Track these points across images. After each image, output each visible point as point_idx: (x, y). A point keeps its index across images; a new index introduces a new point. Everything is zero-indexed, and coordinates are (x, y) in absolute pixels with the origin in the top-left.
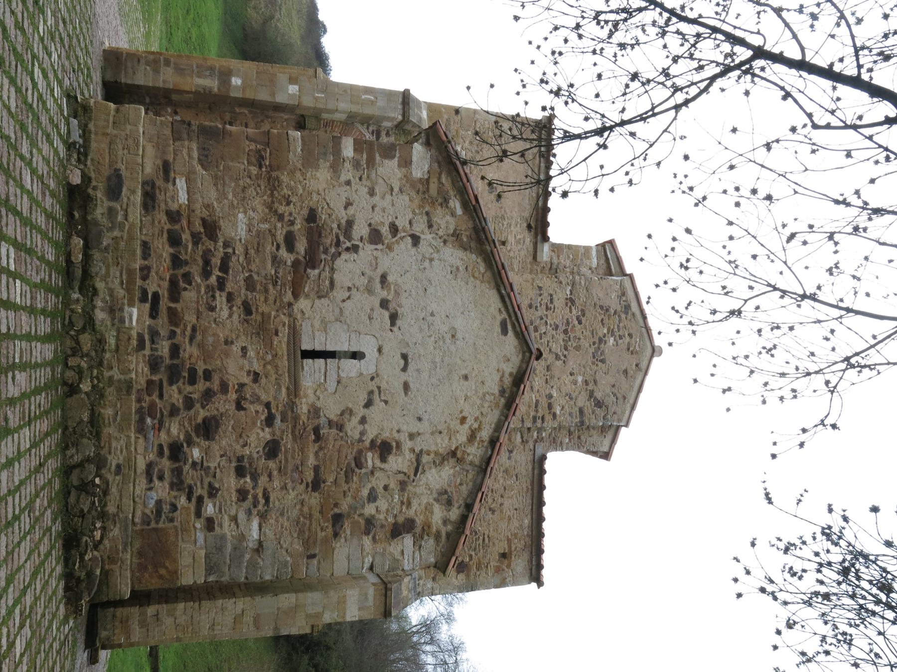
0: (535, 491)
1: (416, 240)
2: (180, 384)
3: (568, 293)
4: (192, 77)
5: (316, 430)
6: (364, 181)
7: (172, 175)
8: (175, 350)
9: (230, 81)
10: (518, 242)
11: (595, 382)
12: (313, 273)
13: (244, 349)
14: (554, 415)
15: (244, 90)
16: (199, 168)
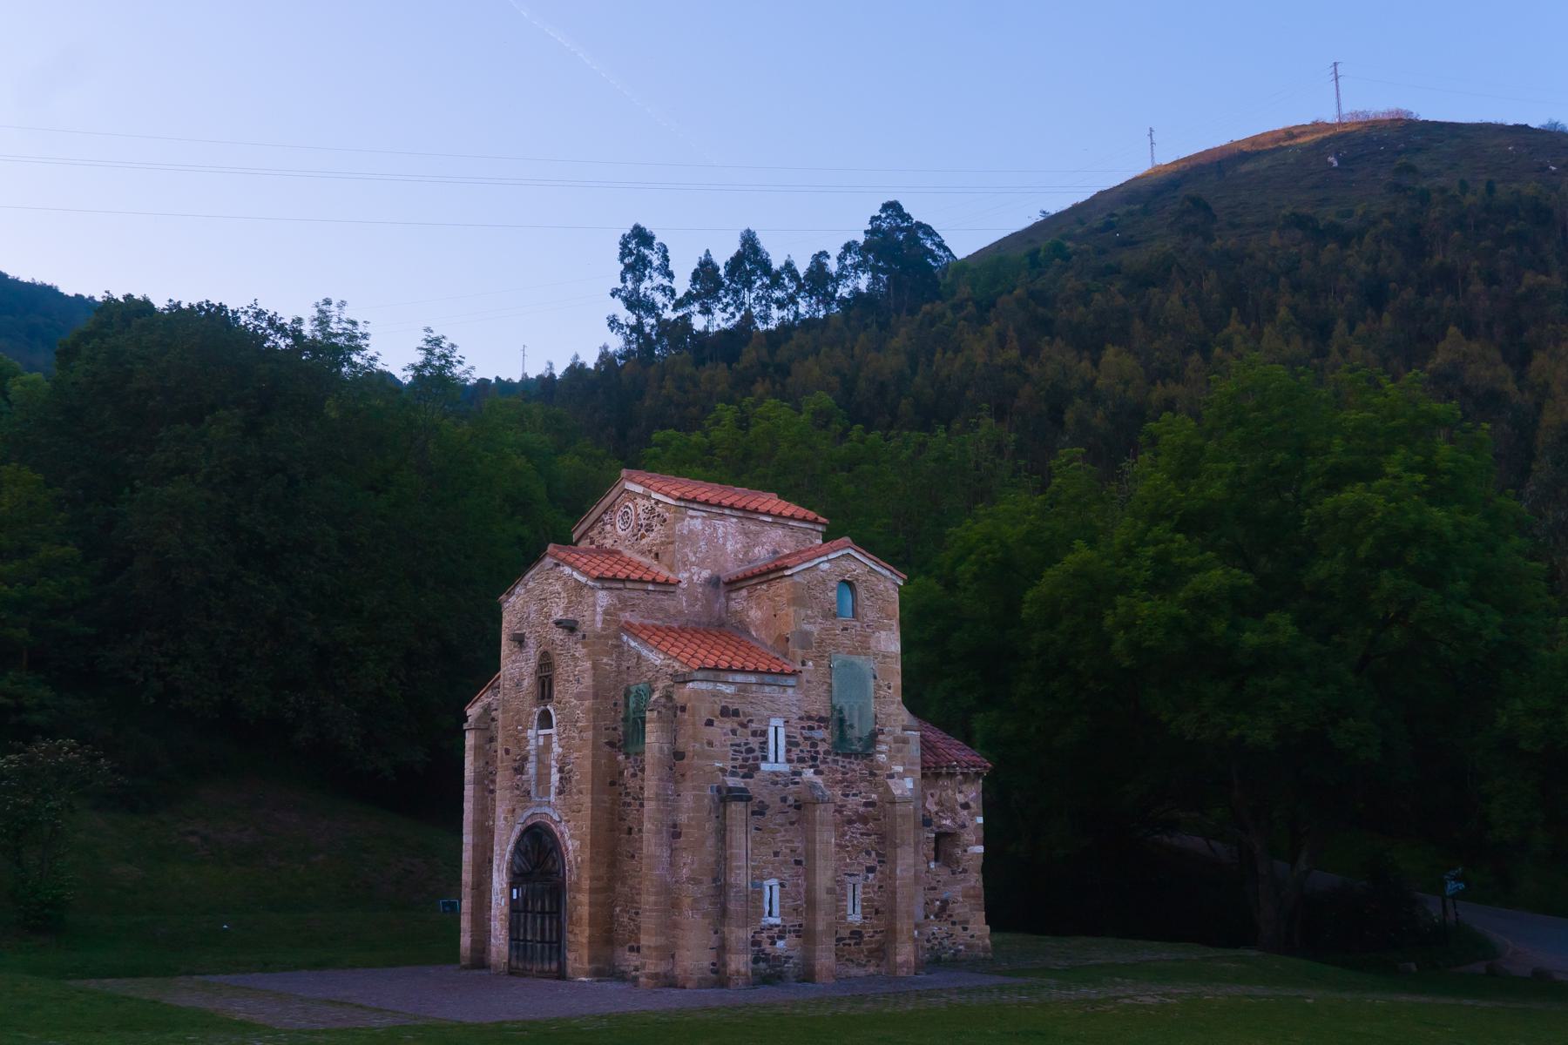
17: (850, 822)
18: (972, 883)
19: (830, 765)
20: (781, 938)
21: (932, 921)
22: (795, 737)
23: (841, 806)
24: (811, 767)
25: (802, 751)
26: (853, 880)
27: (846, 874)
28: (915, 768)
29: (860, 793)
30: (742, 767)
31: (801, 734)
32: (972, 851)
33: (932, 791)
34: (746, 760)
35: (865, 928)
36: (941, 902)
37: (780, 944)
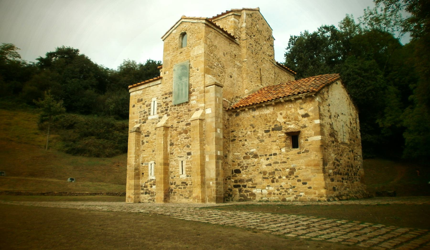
0: (282, 68)
1: (329, 105)
5: (351, 140)
6: (324, 118)
8: (346, 174)
9: (219, 156)
12: (336, 137)
17: (180, 133)
18: (312, 158)
19: (173, 111)
20: (154, 185)
21: (284, 180)
22: (160, 103)
23: (176, 128)
24: (166, 113)
25: (162, 108)
26: (181, 159)
27: (178, 157)
28: (211, 103)
29: (184, 120)
30: (143, 119)
31: (163, 101)
32: (311, 140)
33: (281, 112)
34: (144, 116)
35: (187, 180)
36: (290, 169)
37: (154, 187)
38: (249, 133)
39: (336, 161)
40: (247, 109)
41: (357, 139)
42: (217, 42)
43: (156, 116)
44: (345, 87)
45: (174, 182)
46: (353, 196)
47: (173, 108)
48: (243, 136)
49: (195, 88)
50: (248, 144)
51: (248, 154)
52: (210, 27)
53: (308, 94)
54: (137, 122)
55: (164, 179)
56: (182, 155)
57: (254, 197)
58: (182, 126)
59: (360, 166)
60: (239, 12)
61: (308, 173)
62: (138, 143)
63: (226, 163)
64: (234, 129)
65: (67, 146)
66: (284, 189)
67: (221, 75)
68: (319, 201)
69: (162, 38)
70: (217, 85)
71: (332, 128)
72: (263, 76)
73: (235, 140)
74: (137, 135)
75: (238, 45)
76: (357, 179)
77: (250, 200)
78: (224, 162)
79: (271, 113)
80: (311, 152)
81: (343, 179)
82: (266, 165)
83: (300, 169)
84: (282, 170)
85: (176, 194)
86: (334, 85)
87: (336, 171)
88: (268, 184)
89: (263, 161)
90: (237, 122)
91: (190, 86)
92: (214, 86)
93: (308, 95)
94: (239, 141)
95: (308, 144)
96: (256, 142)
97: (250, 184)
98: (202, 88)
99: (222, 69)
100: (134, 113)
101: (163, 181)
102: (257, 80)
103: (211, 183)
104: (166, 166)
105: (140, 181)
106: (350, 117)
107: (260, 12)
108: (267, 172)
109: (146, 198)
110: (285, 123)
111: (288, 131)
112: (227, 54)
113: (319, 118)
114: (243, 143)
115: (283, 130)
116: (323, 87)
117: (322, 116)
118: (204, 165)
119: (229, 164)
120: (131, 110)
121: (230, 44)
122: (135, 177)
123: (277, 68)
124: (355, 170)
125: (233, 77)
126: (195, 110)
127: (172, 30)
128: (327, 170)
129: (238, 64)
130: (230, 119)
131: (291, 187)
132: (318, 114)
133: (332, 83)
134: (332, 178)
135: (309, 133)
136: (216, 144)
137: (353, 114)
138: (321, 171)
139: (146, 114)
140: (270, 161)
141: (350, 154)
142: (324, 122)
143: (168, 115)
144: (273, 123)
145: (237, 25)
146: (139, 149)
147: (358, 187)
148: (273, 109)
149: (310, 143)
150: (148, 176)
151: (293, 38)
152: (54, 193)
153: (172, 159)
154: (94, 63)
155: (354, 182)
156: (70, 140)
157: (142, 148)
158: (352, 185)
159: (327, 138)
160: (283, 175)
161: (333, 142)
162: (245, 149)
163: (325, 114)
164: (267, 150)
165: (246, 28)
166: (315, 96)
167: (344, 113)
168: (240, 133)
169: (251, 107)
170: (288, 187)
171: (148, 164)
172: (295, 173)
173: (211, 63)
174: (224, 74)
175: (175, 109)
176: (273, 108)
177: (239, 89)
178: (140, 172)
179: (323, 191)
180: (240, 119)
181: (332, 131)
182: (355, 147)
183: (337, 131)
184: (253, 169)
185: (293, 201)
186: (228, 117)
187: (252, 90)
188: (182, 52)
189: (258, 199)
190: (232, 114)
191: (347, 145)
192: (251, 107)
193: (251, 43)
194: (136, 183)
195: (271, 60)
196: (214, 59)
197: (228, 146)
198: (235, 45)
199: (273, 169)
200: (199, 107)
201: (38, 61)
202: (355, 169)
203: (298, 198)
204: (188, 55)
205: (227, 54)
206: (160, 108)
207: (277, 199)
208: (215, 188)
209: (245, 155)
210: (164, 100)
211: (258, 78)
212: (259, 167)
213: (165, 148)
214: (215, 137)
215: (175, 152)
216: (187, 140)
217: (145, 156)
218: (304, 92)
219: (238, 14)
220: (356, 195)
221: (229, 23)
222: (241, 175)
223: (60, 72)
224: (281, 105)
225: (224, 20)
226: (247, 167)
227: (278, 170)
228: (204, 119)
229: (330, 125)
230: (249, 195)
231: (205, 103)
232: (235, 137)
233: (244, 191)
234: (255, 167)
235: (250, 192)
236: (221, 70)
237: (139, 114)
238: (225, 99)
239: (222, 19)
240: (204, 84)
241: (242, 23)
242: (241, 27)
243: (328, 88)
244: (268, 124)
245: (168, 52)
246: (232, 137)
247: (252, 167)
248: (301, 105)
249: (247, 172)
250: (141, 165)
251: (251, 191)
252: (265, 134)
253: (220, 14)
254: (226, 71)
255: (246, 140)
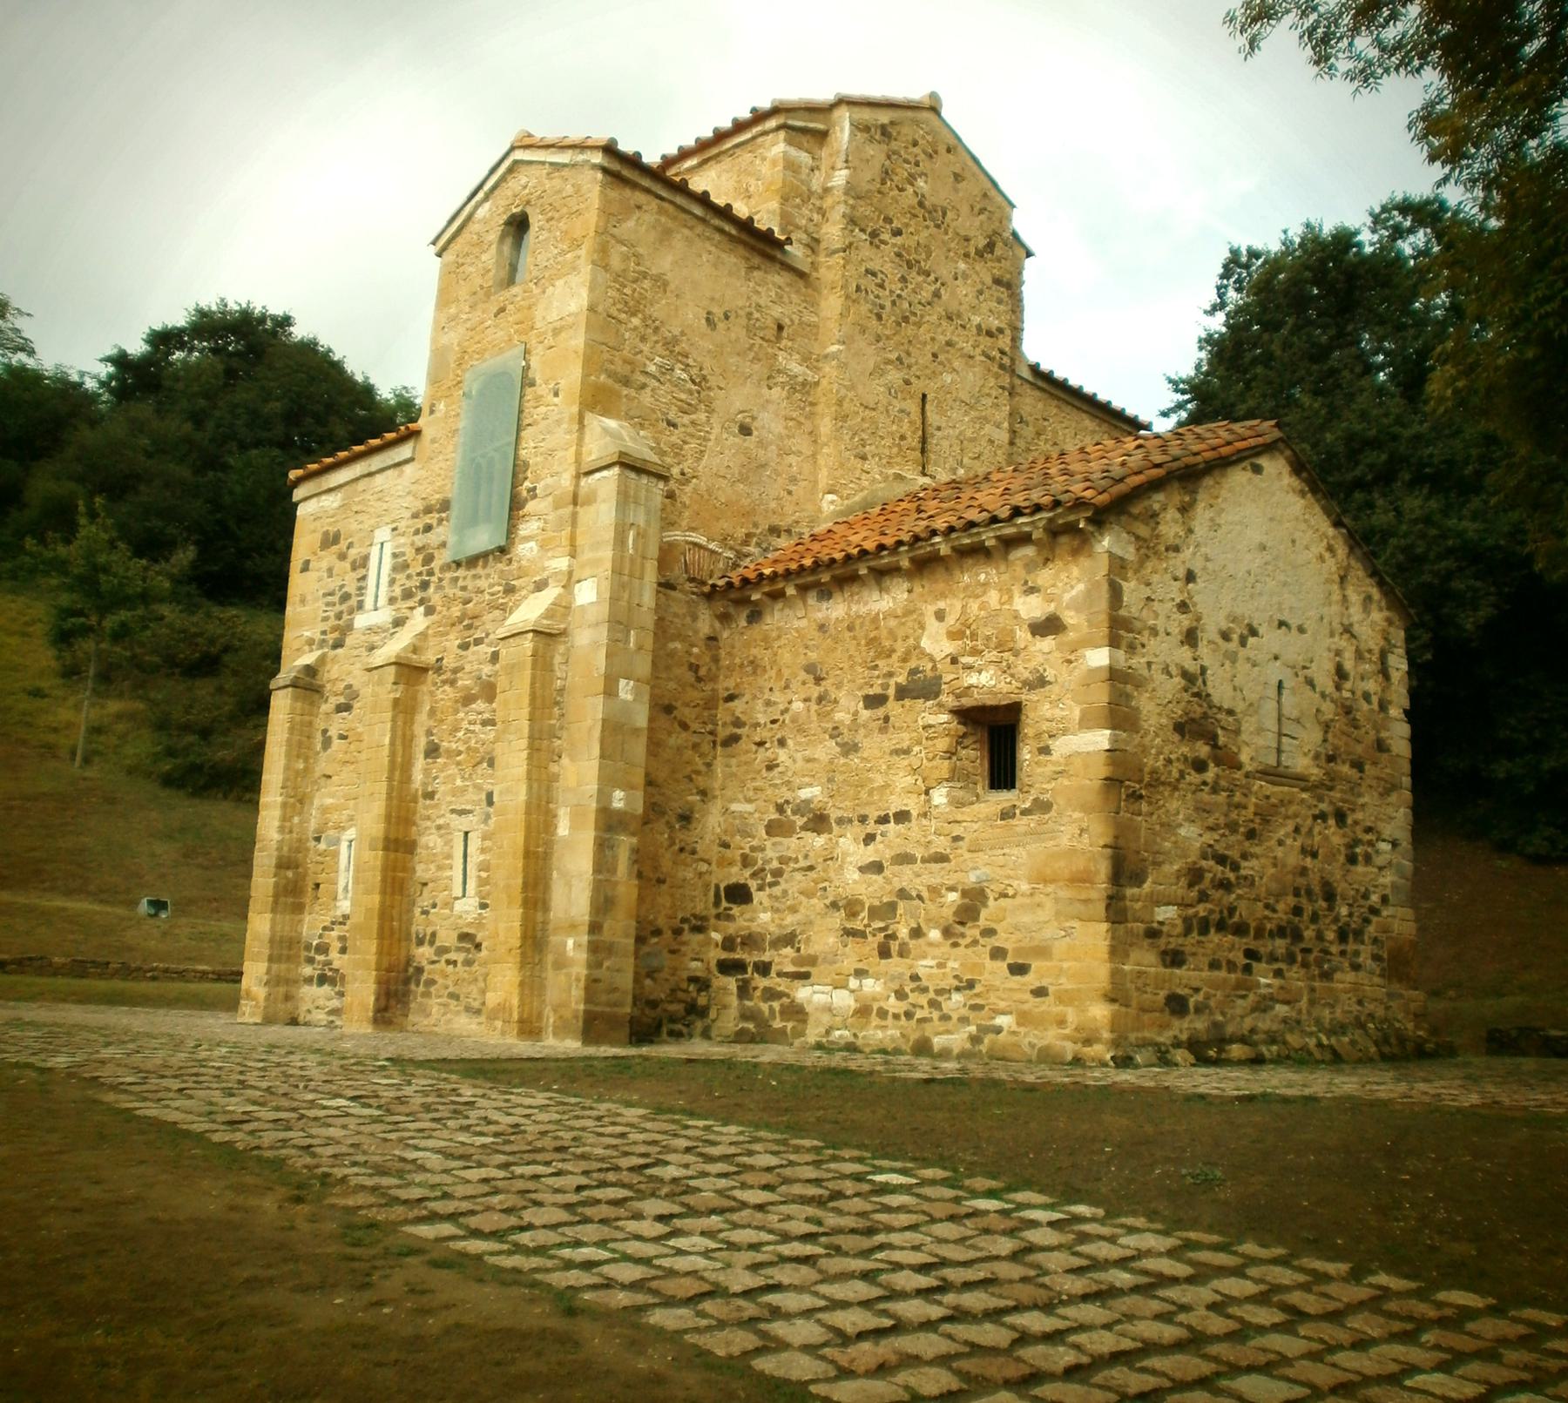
0: (1062, 395)
1: (1190, 577)
2: (1302, 926)
3: (864, 237)
4: (616, 883)
5: (1331, 759)
6: (1144, 640)
7: (1155, 925)
8: (1281, 932)
9: (618, 812)
10: (778, 300)
11: (967, 240)
12: (1222, 740)
13: (1280, 843)
14: (1000, 331)
15: (632, 788)
16: (1147, 886)
17: (468, 700)
18: (1065, 841)
21: (931, 944)
22: (403, 554)
23: (455, 671)
24: (422, 602)
27: (453, 811)
28: (600, 554)
29: (488, 635)
30: (334, 629)
32: (1066, 751)
33: (941, 604)
34: (339, 616)
36: (965, 894)
38: (798, 706)
39: (1212, 863)
40: (791, 591)
41: (1385, 756)
42: (670, 258)
43: (384, 616)
44: (1314, 490)
45: (429, 931)
46: (1312, 1042)
47: (448, 575)
48: (774, 722)
49: (538, 479)
50: (789, 763)
51: (789, 812)
52: (634, 186)
53: (1059, 516)
54: (310, 642)
55: (385, 915)
56: (468, 802)
57: (800, 1027)
58: (476, 662)
59: (1388, 891)
60: (821, 116)
61: (1043, 915)
62: (301, 746)
63: (682, 850)
64: (737, 685)
65: (170, 753)
66: (925, 990)
67: (686, 419)
68: (1077, 1061)
69: (434, 243)
70: (628, 464)
71: (1197, 695)
72: (939, 429)
73: (735, 739)
74: (299, 704)
75: (802, 275)
76: (1365, 958)
77: (780, 1037)
78: (672, 843)
79: (899, 612)
80: (1060, 814)
81: (1251, 954)
82: (862, 869)
83: (1006, 896)
84: (925, 894)
85: (432, 989)
86: (1239, 477)
87: (1202, 914)
88: (860, 966)
89: (849, 845)
90: (754, 651)
91: (518, 470)
92: (616, 470)
93: (1061, 521)
94: (754, 748)
95: (1051, 768)
96: (826, 750)
97: (784, 959)
98: (566, 481)
99: (690, 392)
100: (303, 601)
101: (376, 921)
102: (895, 450)
103: (570, 943)
104: (399, 855)
105: (300, 921)
106: (1342, 642)
107: (944, 114)
108: (862, 903)
109: (321, 1002)
110: (954, 661)
111: (967, 702)
112: (727, 317)
113: (1106, 641)
114: (769, 754)
115: (943, 698)
116: (1155, 485)
117: (1130, 631)
118: (547, 856)
119: (701, 854)
120: (298, 584)
121: (752, 268)
122: (276, 902)
123: (1037, 393)
124: (1350, 915)
125: (755, 433)
126: (532, 587)
127: (473, 202)
128: (1138, 905)
129: (796, 368)
130: (725, 634)
131: (956, 983)
132: (1103, 618)
133: (1222, 464)
134: (1171, 946)
135: (1058, 713)
136: (602, 756)
137: (1363, 631)
138: (1100, 909)
139: (349, 601)
140: (877, 851)
141: (1316, 830)
142: (1138, 662)
143: (430, 611)
144: (904, 660)
145: (803, 177)
146: (306, 770)
147: (1360, 1002)
148: (910, 591)
149: (1057, 763)
150: (335, 899)
151: (1244, 259)
152: (50, 964)
153: (429, 823)
154: (359, 378)
155: (1338, 976)
156: (186, 728)
157: (322, 765)
158: (1313, 990)
159: (1158, 741)
160: (929, 920)
161: (1200, 766)
162: (775, 786)
163: (1151, 622)
164: (871, 793)
165: (846, 193)
166: (1090, 528)
167: (1294, 622)
168: (759, 705)
169: (810, 579)
170: (944, 985)
171: (337, 842)
172: (984, 914)
173: (625, 361)
174: (702, 416)
175: (456, 579)
176: (906, 585)
177: (790, 493)
178: (305, 875)
179: (1100, 1012)
180: (766, 639)
181: (1197, 711)
182: (1360, 795)
183: (1230, 712)
184: (803, 885)
185: (963, 1055)
186: (712, 626)
187: (865, 499)
188: (502, 310)
189: (813, 1035)
190: (732, 610)
191: (1303, 784)
192: (810, 579)
193: (875, 265)
194: (278, 928)
195: (995, 353)
196: (643, 339)
197: (703, 769)
198: (780, 278)
199: (888, 888)
200: (545, 575)
201: (111, 369)
202: (1350, 905)
203: (986, 1041)
204: (525, 325)
205: (727, 317)
206: (401, 577)
207: (893, 1039)
208: (584, 972)
209: (775, 816)
210: (420, 540)
211: (903, 438)
212: (832, 874)
213: (400, 768)
214: (604, 721)
215: (442, 788)
216: (489, 734)
217: (329, 801)
218: (1038, 508)
219: (812, 125)
220: (1333, 1041)
221: (765, 169)
222: (755, 911)
223: (198, 419)
224: (940, 573)
225: (745, 157)
226: (778, 873)
227: (910, 898)
228: (564, 633)
229: (1185, 674)
230: (782, 1013)
231: (573, 556)
232: (738, 723)
233: (758, 993)
234: (812, 875)
235: (785, 1000)
236: (683, 396)
237: (321, 604)
238: (702, 540)
239: (738, 152)
240: (578, 461)
241: (833, 168)
242: (827, 190)
243: (1195, 492)
244: (880, 663)
245: (453, 310)
246: (724, 724)
247: (798, 876)
248: (1029, 572)
249: (777, 898)
250: (314, 843)
251: (788, 996)
252: (865, 714)
253: (727, 124)
254: (717, 404)
255: (782, 743)
